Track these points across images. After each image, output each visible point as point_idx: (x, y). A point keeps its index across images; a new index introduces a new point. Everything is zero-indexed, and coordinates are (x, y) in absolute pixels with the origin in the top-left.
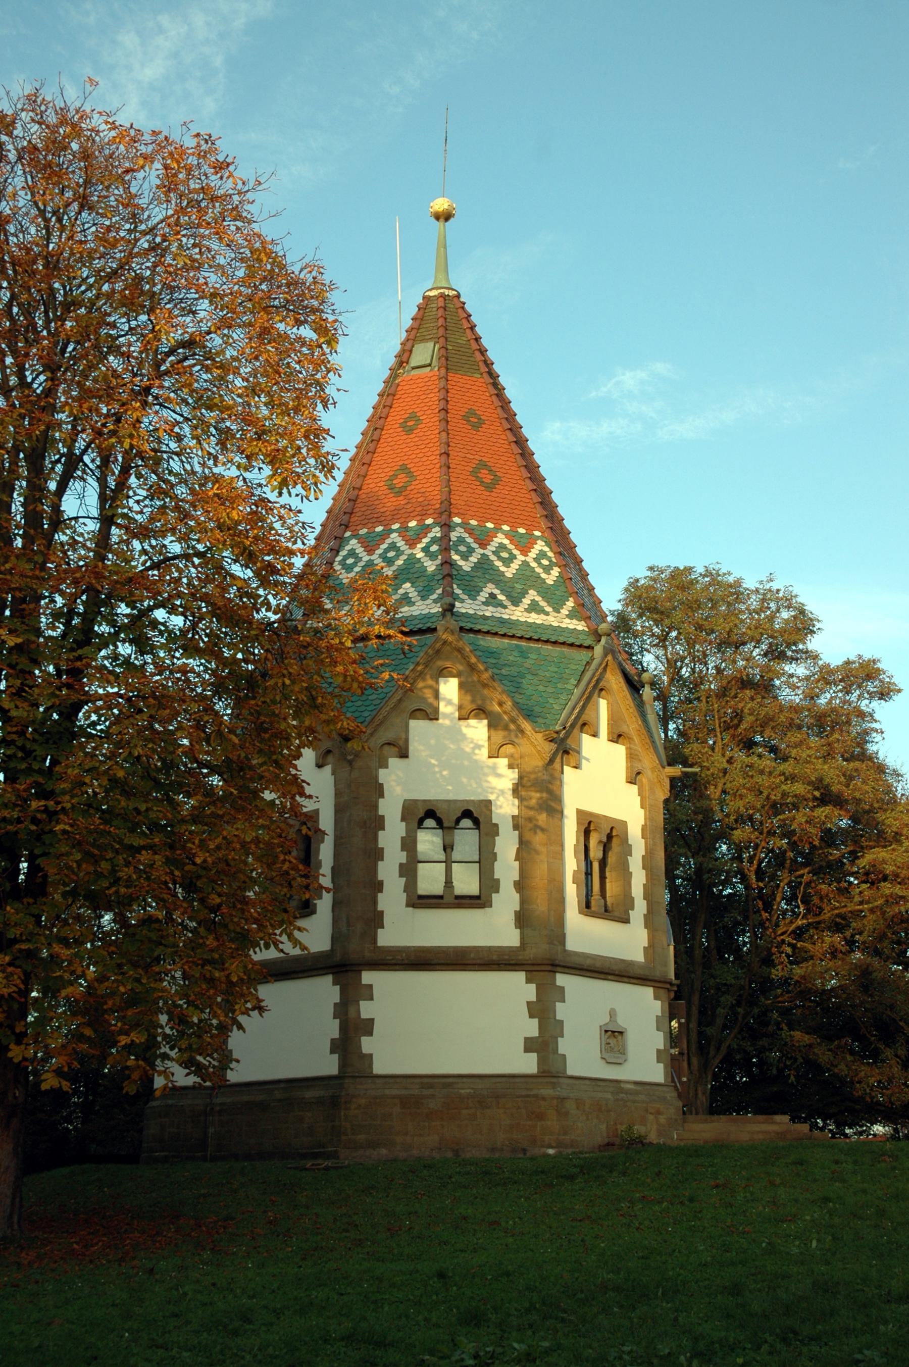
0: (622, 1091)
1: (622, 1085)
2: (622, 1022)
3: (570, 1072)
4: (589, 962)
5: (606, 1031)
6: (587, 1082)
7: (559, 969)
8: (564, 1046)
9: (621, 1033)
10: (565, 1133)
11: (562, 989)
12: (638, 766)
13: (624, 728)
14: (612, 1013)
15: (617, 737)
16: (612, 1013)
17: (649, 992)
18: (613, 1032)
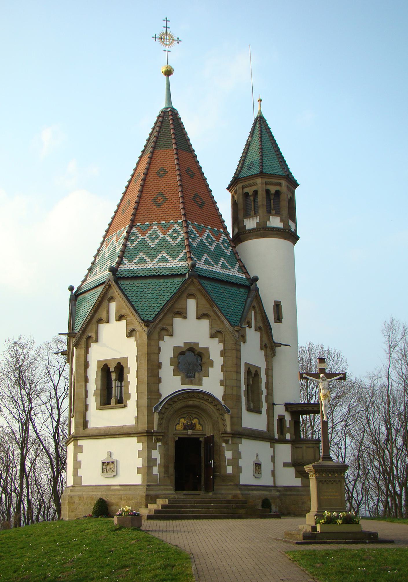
0: (109, 490)
1: (112, 488)
2: (115, 457)
3: (84, 483)
4: (97, 431)
5: (103, 463)
6: (91, 488)
7: (78, 439)
8: (80, 472)
9: (113, 462)
10: (72, 511)
11: (81, 447)
12: (132, 327)
13: (123, 312)
14: (110, 454)
15: (120, 318)
16: (110, 454)
17: (135, 439)
18: (108, 463)
